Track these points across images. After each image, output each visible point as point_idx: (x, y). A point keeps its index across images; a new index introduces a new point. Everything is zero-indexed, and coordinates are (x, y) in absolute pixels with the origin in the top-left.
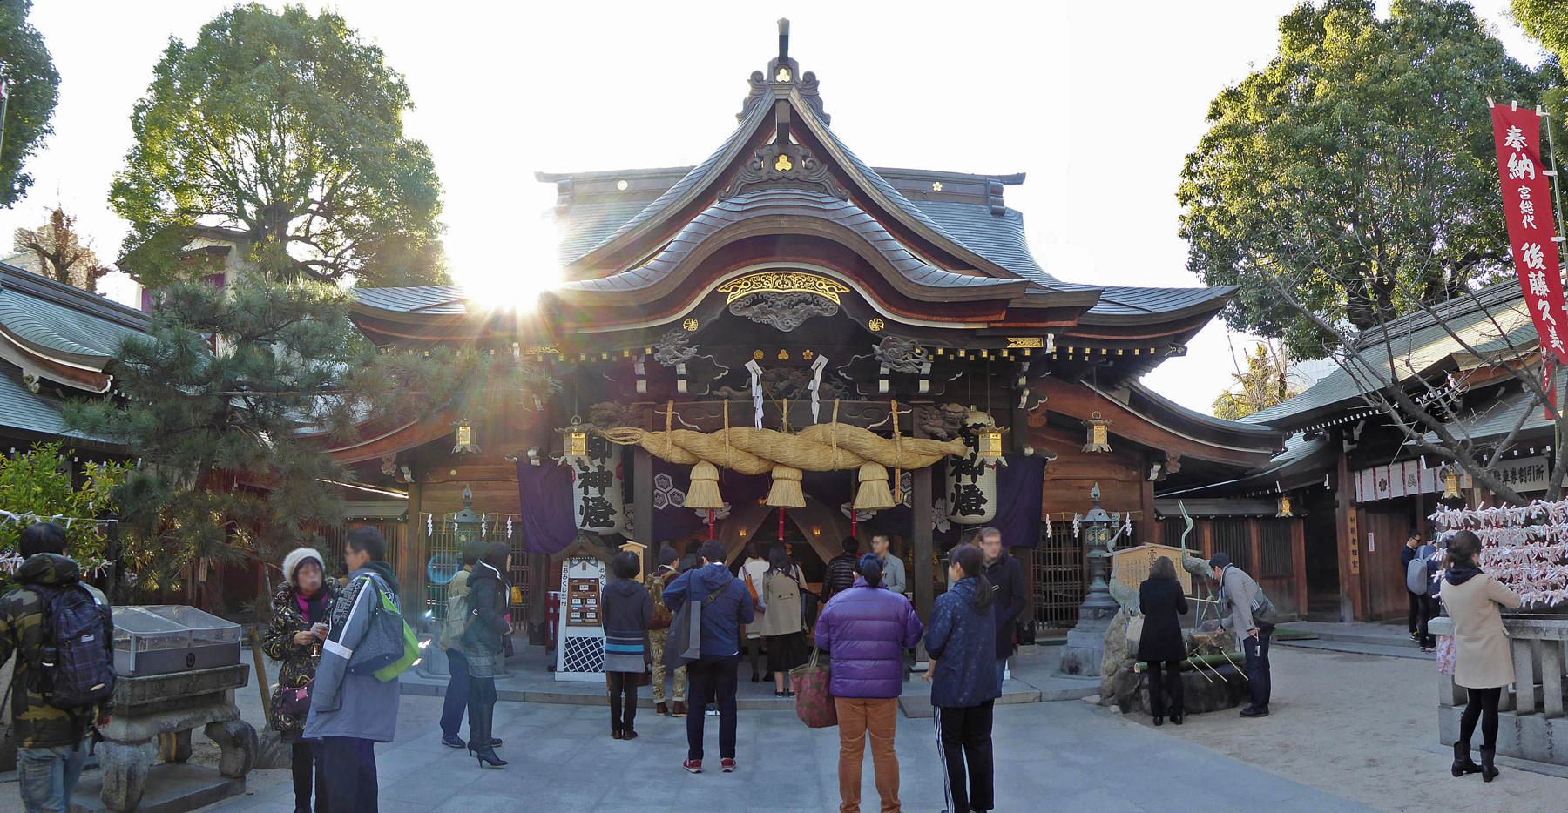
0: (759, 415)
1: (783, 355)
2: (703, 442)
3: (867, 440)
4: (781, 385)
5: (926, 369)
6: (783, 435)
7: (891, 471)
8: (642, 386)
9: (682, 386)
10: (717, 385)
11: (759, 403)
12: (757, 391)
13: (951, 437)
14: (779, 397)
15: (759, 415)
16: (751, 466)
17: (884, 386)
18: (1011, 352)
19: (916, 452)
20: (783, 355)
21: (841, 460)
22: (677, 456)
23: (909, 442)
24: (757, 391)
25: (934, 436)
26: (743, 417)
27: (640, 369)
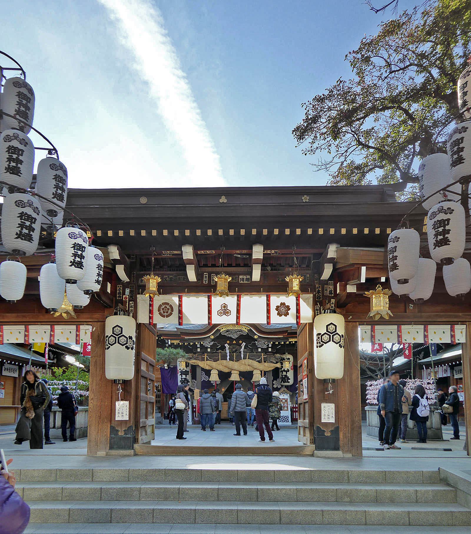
0: (228, 357)
1: (234, 342)
2: (214, 364)
3: (255, 364)
4: (234, 350)
5: (270, 346)
6: (234, 362)
7: (261, 371)
8: (199, 350)
9: (209, 350)
10: (217, 350)
11: (228, 354)
12: (228, 351)
13: (277, 363)
14: (233, 352)
15: (228, 357)
16: (226, 370)
17: (260, 350)
18: (290, 342)
19: (269, 366)
20: (234, 342)
21: (249, 369)
22: (207, 368)
23: (266, 364)
24: (228, 351)
25: (272, 362)
26: (224, 358)
27: (198, 346)
